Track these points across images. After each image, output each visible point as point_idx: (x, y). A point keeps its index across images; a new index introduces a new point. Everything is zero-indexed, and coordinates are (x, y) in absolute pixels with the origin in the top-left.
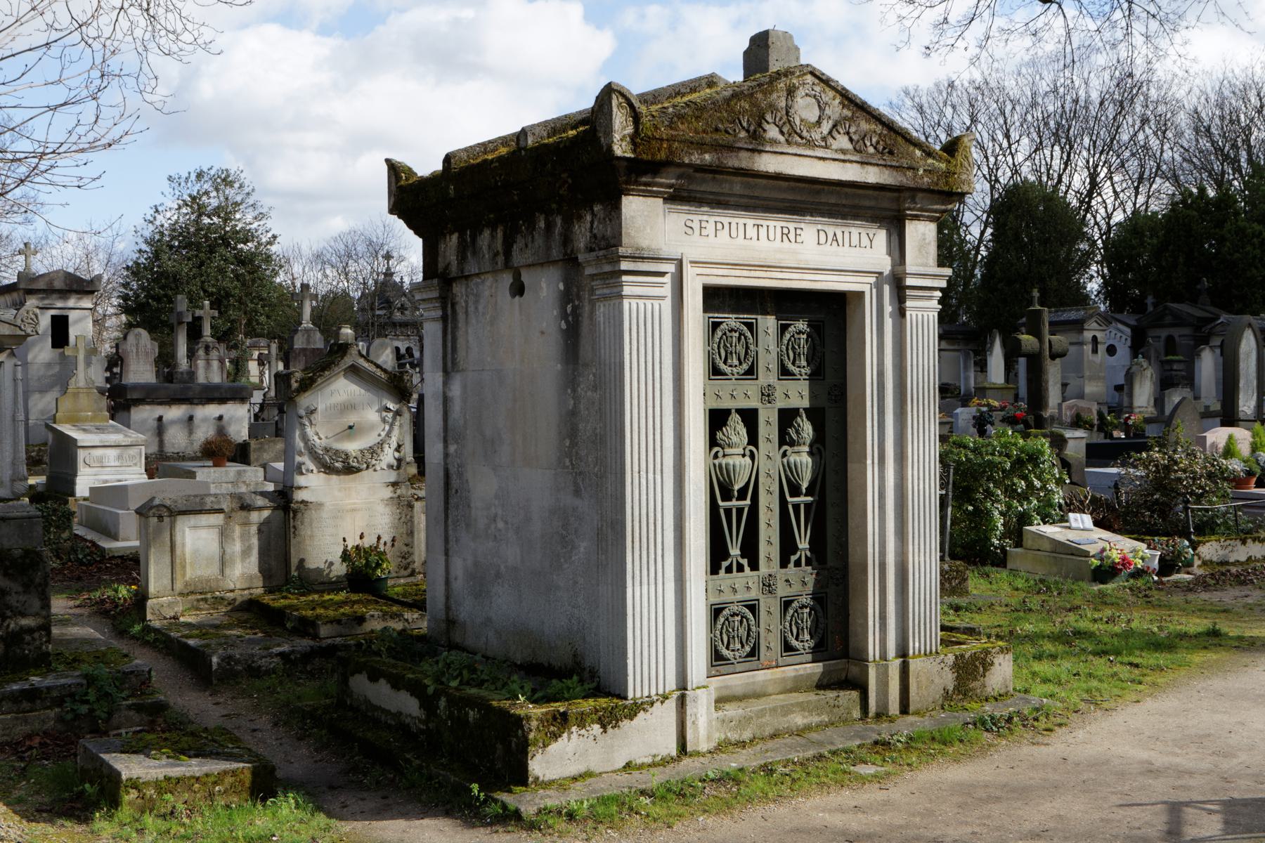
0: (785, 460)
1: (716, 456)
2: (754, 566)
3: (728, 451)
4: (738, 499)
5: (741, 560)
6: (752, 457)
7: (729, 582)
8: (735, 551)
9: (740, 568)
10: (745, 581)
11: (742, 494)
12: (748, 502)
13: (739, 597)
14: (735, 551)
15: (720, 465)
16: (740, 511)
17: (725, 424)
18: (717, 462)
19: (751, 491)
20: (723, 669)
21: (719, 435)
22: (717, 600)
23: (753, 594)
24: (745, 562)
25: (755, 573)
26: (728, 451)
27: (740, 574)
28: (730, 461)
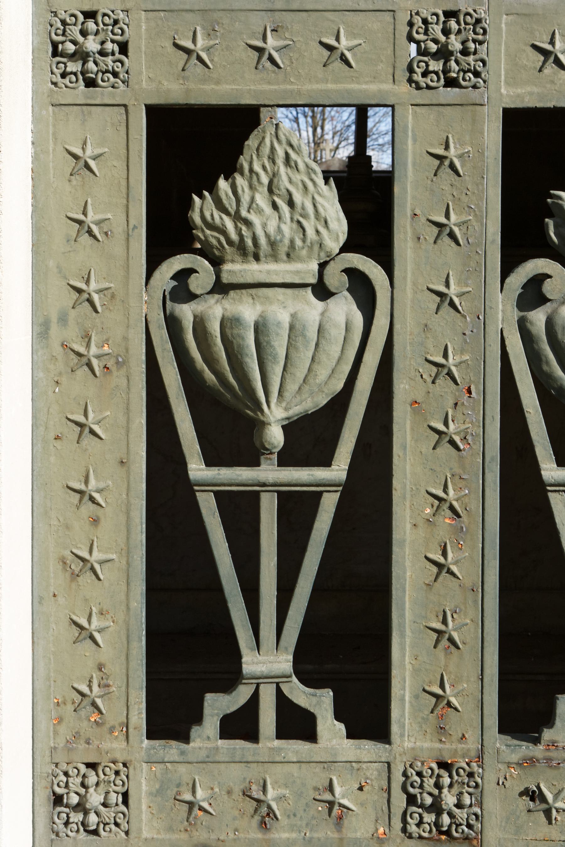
0: (538, 318)
1: (181, 291)
2: (368, 718)
3: (236, 269)
4: (286, 459)
5: (300, 695)
6: (362, 291)
7: (235, 775)
8: (268, 659)
9: (297, 724)
10: (316, 777)
11: (311, 438)
12: (339, 470)
14: (268, 659)
15: (200, 325)
16: (297, 508)
17: (230, 169)
18: (186, 312)
19: (358, 428)
21: (202, 208)
24: (320, 703)
25: (367, 749)
26: (236, 269)
27: (296, 748)
28: (247, 310)
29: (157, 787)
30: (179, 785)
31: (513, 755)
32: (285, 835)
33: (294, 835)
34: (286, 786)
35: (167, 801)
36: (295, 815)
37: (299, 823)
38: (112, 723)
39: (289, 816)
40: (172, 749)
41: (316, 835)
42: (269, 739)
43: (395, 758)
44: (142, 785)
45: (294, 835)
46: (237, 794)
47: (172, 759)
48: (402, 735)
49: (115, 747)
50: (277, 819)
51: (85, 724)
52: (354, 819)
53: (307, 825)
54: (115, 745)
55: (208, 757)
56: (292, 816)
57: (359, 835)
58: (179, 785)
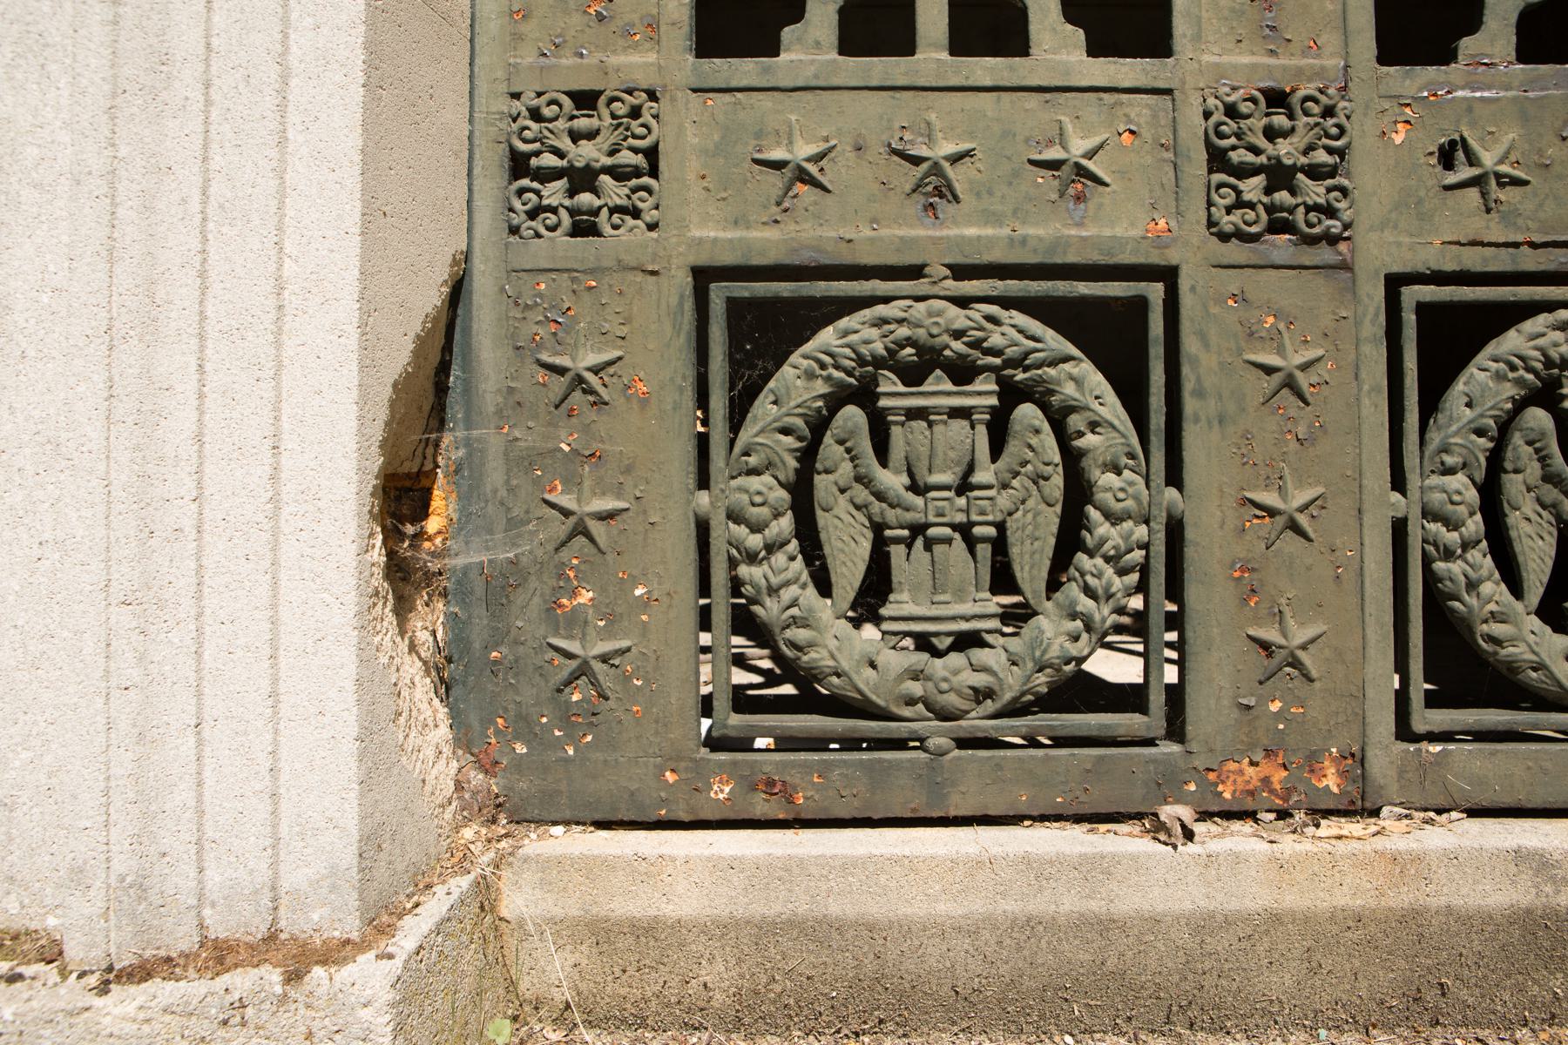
13: (970, 231)
20: (810, 775)
22: (766, 241)
23: (1120, 224)
29: (716, 137)
30: (759, 135)
31: (1408, 82)
32: (972, 231)
33: (989, 231)
34: (971, 135)
35: (736, 165)
36: (990, 193)
37: (999, 207)
38: (627, 18)
39: (978, 194)
40: (745, 69)
41: (1031, 231)
42: (936, 46)
43: (1184, 83)
44: (685, 130)
45: (989, 231)
46: (876, 150)
47: (744, 83)
48: (1198, 38)
49: (635, 63)
50: (956, 199)
51: (576, 20)
52: (1106, 201)
53: (1015, 212)
54: (635, 58)
55: (816, 76)
56: (985, 196)
57: (1119, 231)
58: (759, 135)
